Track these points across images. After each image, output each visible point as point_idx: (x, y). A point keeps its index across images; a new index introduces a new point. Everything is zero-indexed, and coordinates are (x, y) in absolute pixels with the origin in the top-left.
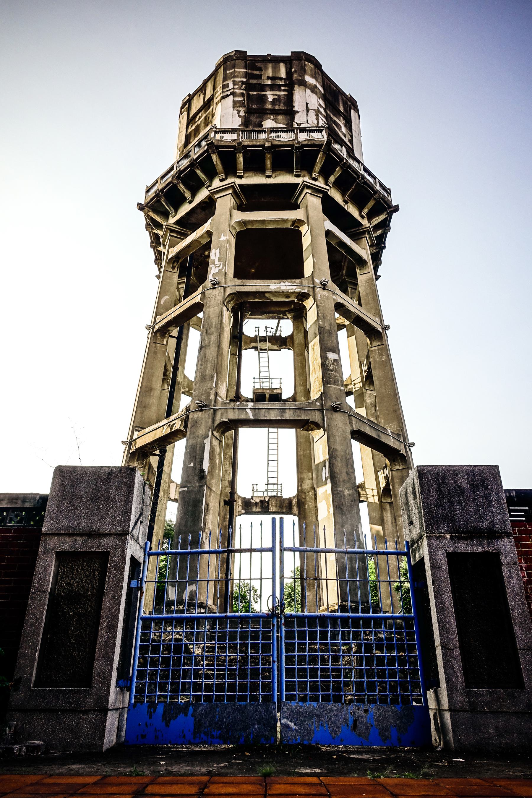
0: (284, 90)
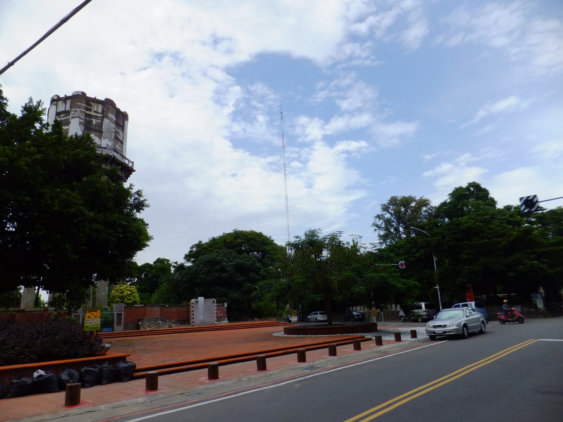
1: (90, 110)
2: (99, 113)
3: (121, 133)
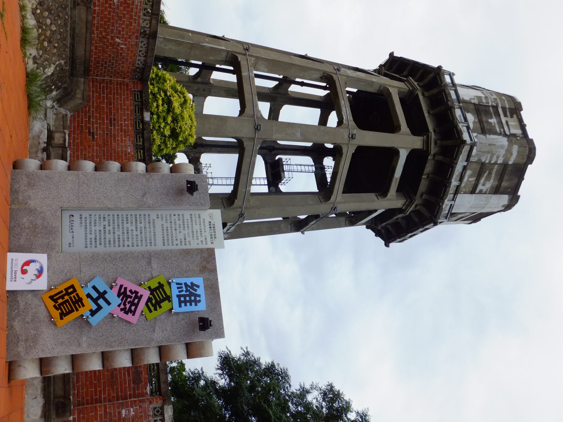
0: (500, 130)
1: (506, 115)
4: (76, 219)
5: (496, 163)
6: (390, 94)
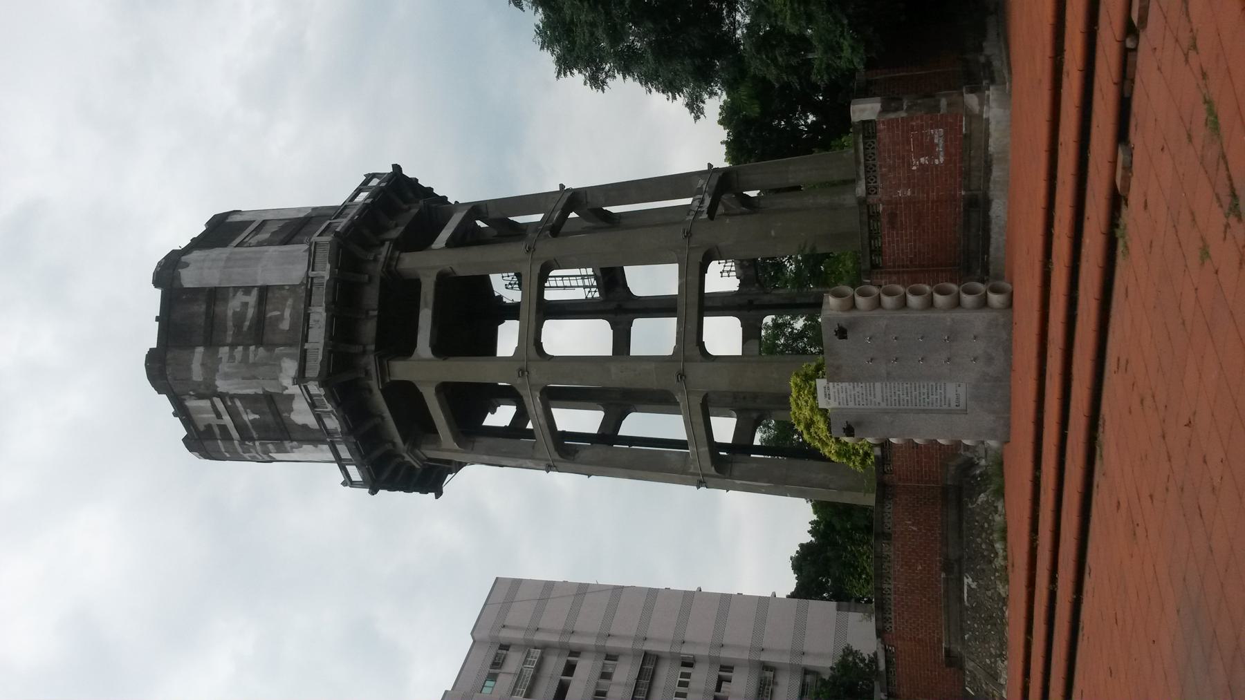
0: (233, 403)
1: (223, 428)
2: (213, 405)
3: (235, 304)
4: (953, 404)
5: (233, 346)
6: (456, 438)
